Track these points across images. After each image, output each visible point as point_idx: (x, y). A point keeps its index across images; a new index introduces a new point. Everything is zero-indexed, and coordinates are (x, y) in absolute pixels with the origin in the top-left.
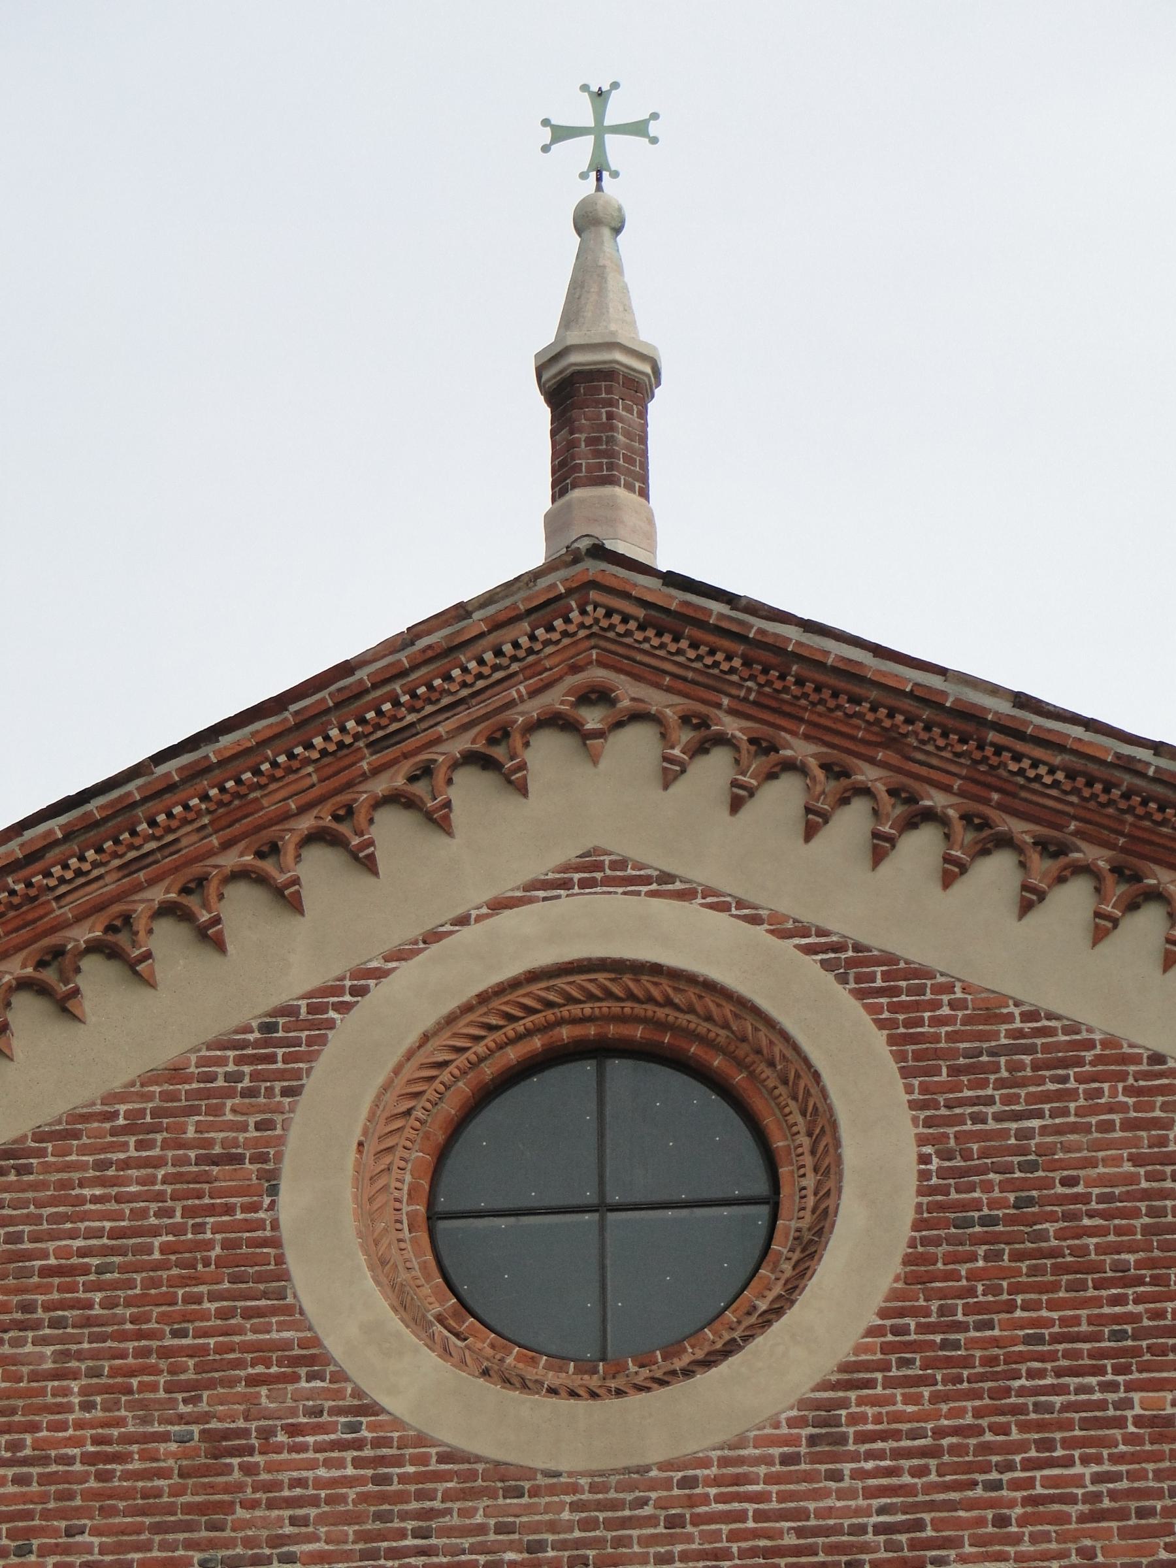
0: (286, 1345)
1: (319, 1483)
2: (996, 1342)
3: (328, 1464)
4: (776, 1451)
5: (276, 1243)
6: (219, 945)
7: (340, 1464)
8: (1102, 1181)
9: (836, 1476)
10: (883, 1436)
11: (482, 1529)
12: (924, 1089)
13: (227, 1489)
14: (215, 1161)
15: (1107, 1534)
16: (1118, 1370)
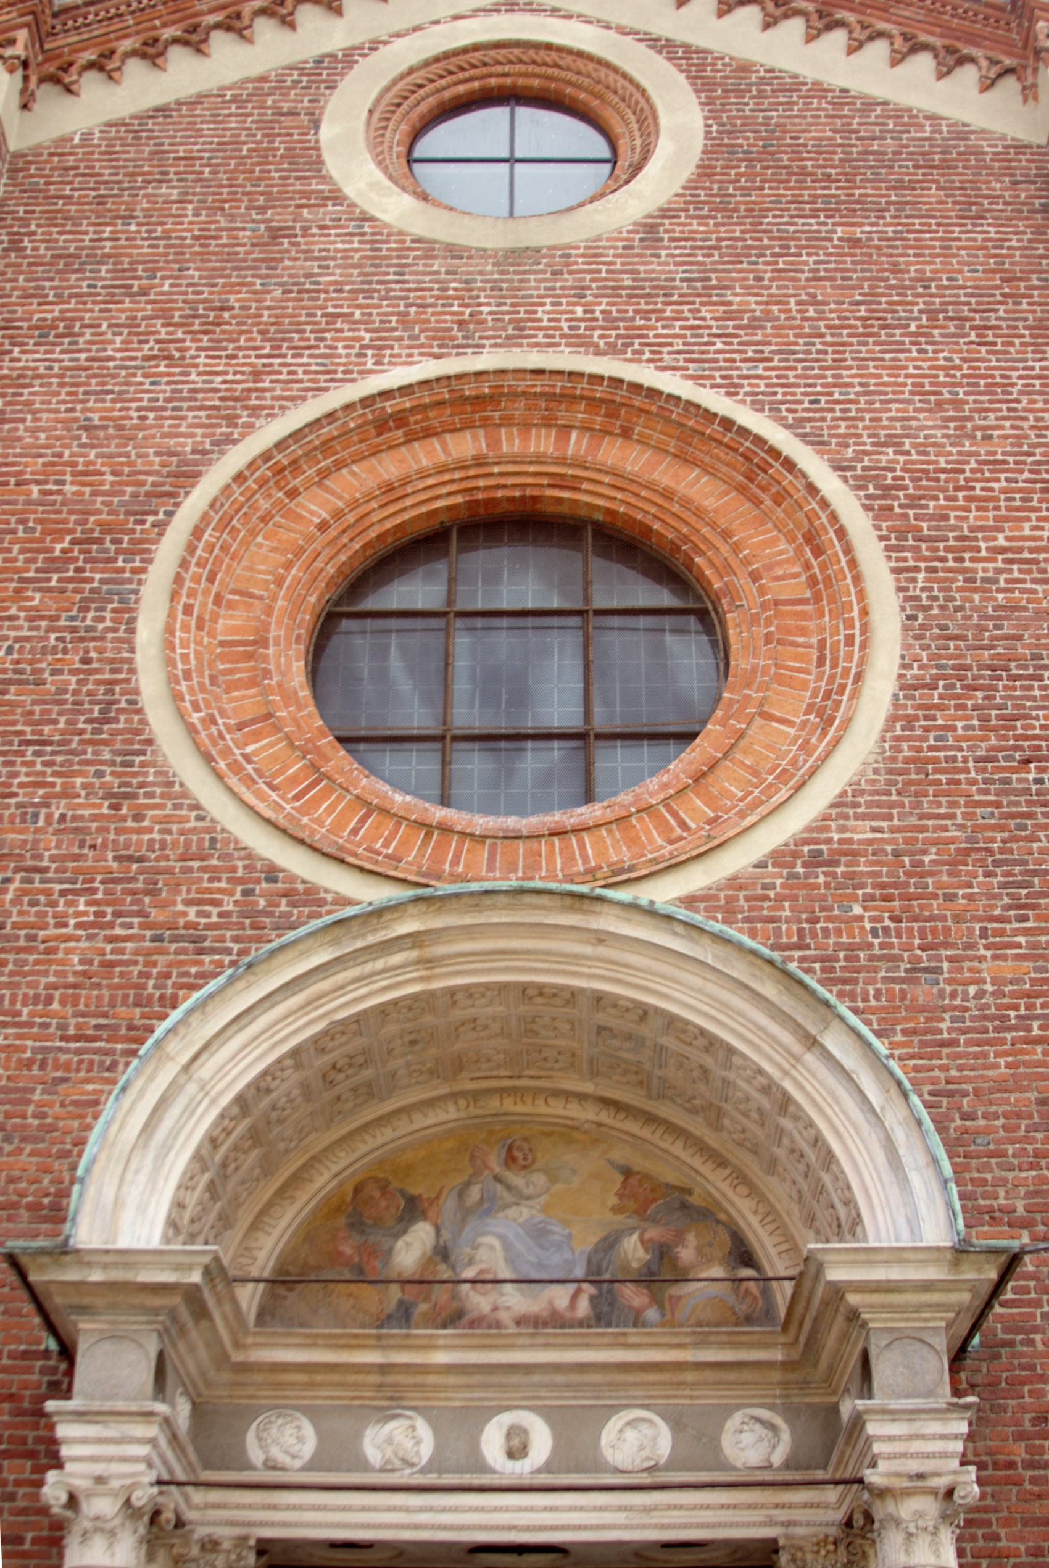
0: (322, 191)
1: (337, 251)
2: (754, 203)
3: (343, 242)
4: (620, 244)
5: (318, 149)
6: (292, 26)
7: (352, 242)
8: (814, 139)
9: (658, 256)
10: (686, 240)
11: (437, 273)
12: (707, 97)
13: (279, 252)
14: (282, 115)
15: (824, 288)
16: (827, 217)
